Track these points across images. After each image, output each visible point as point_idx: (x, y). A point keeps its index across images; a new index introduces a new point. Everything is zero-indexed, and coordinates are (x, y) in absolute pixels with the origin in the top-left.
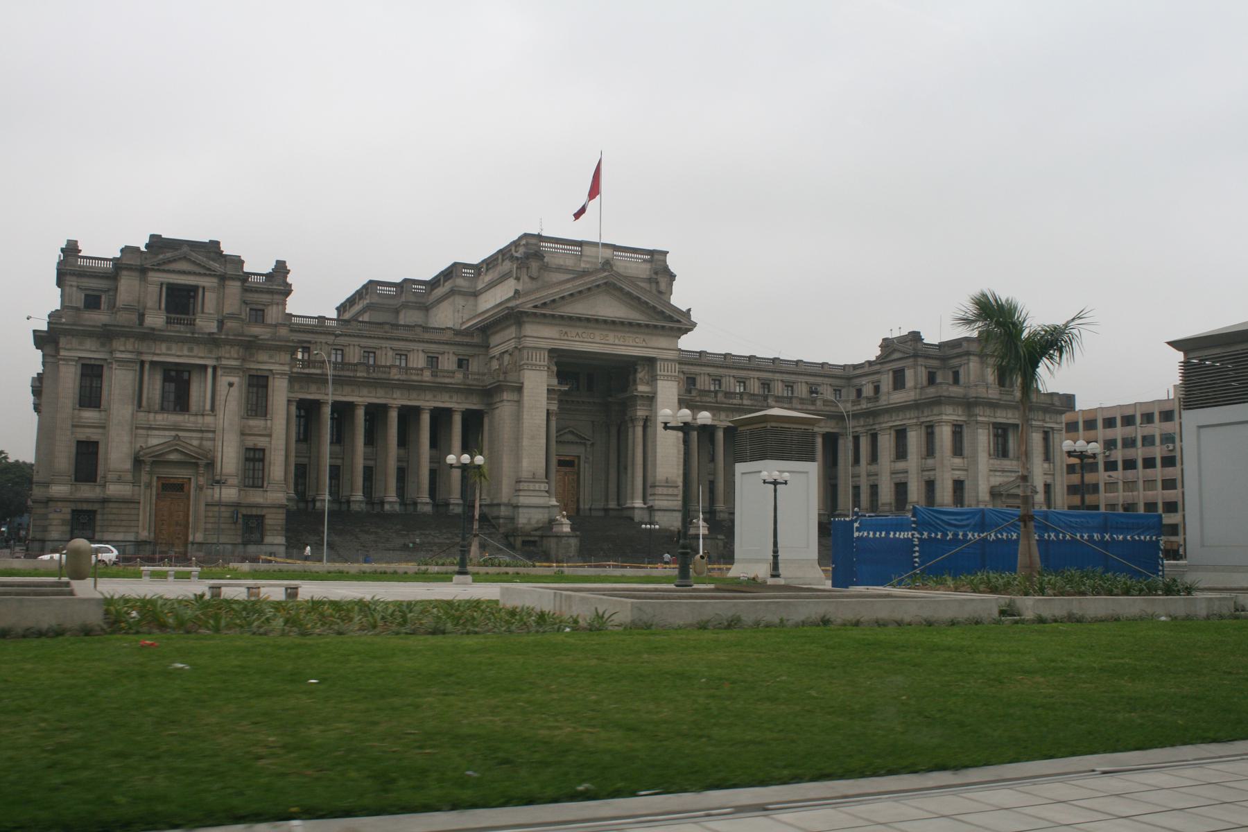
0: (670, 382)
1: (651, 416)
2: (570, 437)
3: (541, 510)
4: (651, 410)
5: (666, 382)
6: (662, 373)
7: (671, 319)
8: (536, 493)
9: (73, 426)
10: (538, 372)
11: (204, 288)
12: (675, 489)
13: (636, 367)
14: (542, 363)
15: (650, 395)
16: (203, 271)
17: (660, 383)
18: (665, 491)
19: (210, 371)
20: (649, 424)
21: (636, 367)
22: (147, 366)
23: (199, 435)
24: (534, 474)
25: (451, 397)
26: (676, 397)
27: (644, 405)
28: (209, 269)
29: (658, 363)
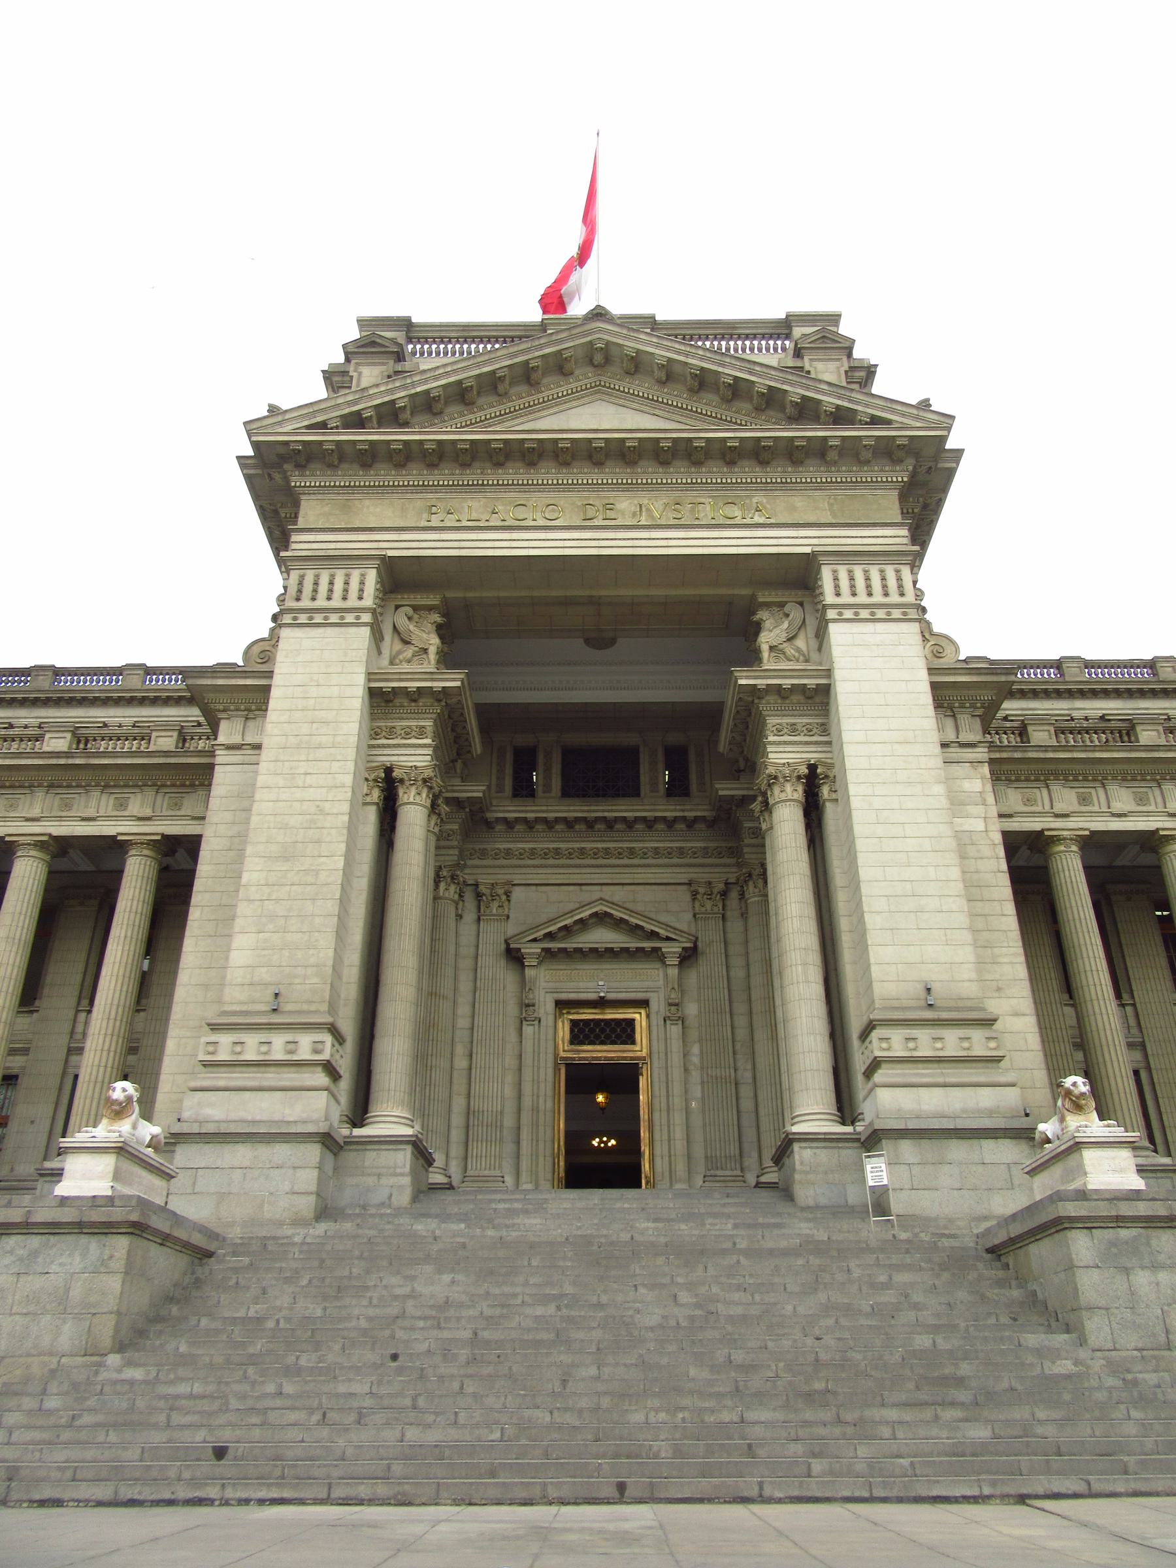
0: (880, 626)
1: (825, 764)
2: (602, 937)
3: (282, 1151)
4: (829, 743)
5: (869, 627)
6: (846, 598)
7: (841, 417)
8: (270, 1077)
10: (337, 629)
12: (977, 1035)
13: (756, 618)
14: (353, 602)
15: (811, 682)
17: (837, 633)
18: (925, 1043)
20: (825, 791)
21: (756, 618)
24: (277, 995)
25: (122, 805)
26: (923, 675)
27: (793, 730)
29: (826, 574)
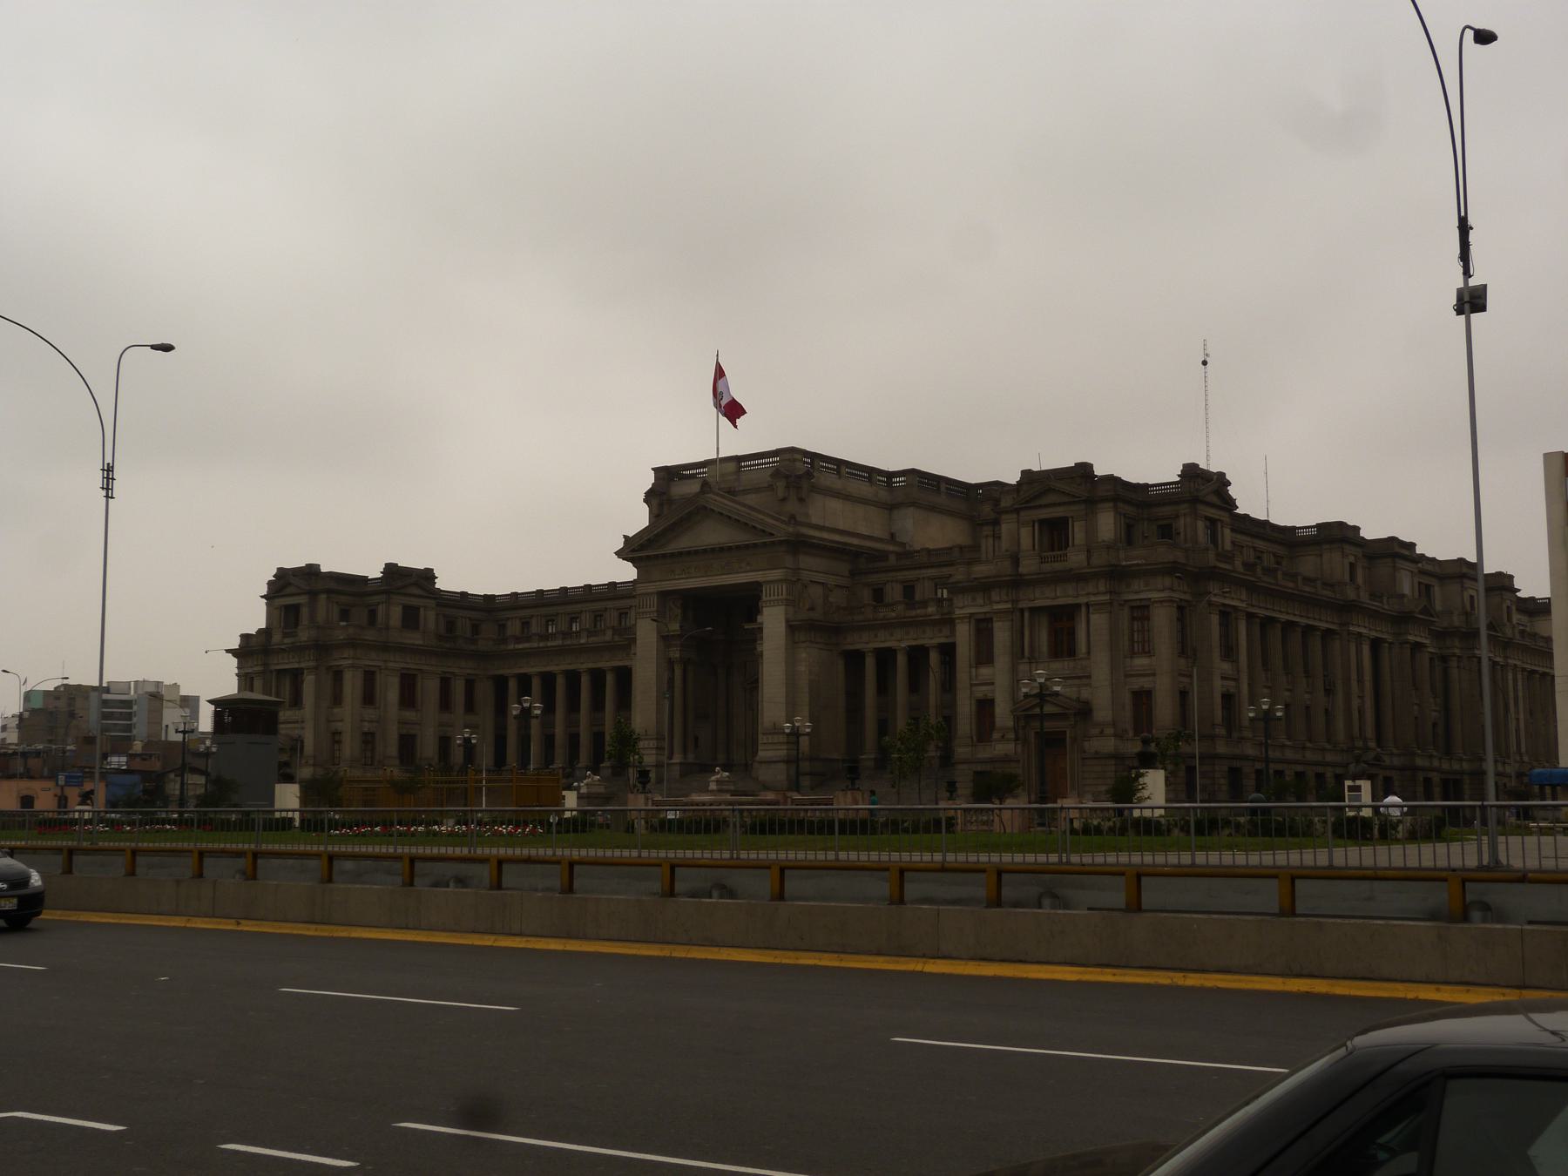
9: (971, 685)
11: (1072, 517)
16: (1066, 499)
19: (1084, 609)
22: (1026, 615)
23: (1077, 682)
28: (1074, 496)
